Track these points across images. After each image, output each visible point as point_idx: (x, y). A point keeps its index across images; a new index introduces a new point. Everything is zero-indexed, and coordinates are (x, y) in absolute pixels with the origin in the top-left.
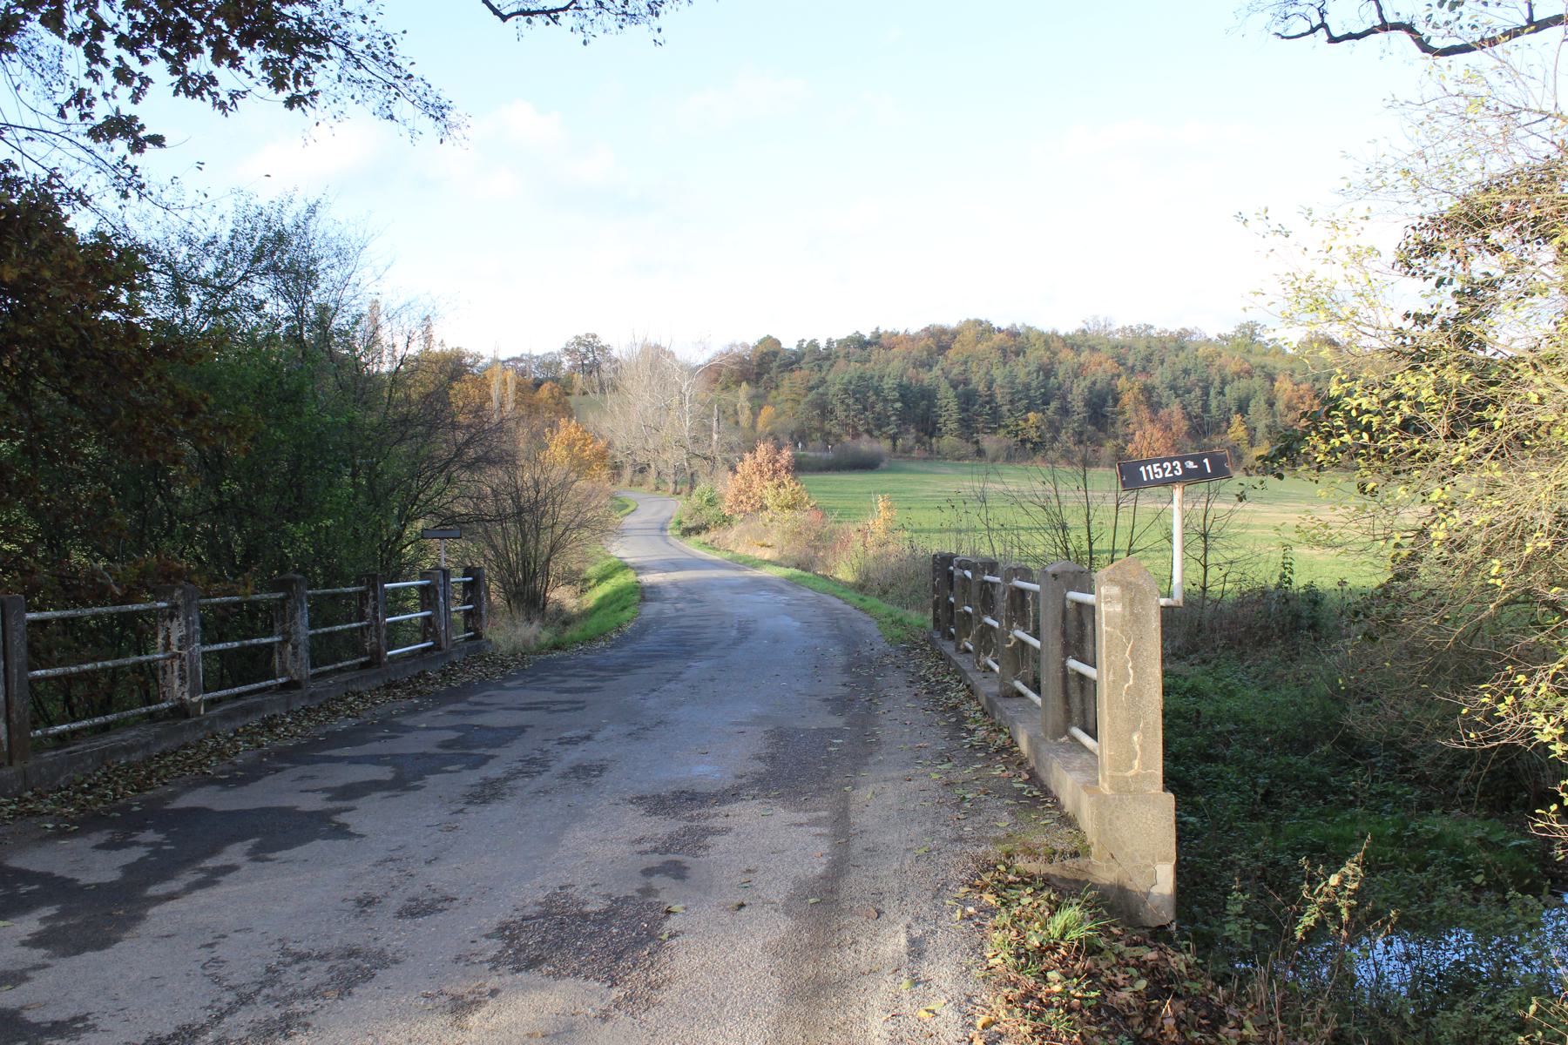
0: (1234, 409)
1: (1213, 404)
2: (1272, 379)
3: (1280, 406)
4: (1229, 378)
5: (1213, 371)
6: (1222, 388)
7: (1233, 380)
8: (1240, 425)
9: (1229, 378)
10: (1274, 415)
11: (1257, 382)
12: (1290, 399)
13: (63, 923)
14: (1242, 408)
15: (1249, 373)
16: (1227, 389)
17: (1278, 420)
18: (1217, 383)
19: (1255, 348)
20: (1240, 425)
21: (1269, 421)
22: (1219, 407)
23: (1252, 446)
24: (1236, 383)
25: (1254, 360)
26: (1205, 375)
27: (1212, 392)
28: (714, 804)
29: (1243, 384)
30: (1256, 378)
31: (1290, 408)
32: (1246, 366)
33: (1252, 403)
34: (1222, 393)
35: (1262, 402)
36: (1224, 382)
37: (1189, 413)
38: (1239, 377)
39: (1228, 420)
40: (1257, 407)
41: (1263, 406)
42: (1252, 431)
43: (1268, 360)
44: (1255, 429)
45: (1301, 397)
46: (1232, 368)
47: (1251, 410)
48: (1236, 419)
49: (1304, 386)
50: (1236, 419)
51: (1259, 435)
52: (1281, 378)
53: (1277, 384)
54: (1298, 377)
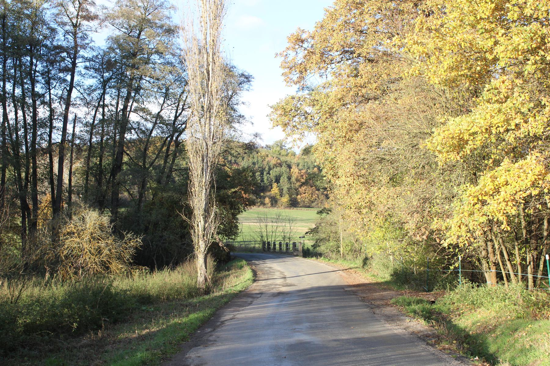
0: (274, 180)
1: (265, 178)
2: (289, 167)
3: (293, 179)
4: (272, 167)
5: (265, 163)
6: (269, 172)
7: (274, 168)
8: (276, 188)
9: (272, 167)
10: (291, 183)
11: (284, 168)
12: (298, 177)
13: (32, 164)
14: (277, 180)
15: (280, 165)
16: (271, 172)
17: (292, 185)
18: (267, 169)
19: (283, 152)
20: (276, 188)
21: (288, 186)
22: (267, 180)
23: (281, 197)
24: (275, 169)
25: (283, 159)
26: (262, 165)
27: (265, 173)
28: (212, 176)
29: (278, 169)
30: (283, 167)
31: (298, 180)
32: (279, 161)
33: (282, 178)
34: (269, 173)
35: (286, 178)
36: (270, 169)
37: (122, 342)
38: (276, 166)
39: (271, 185)
40: (284, 180)
41: (286, 179)
42: (281, 190)
43: (288, 159)
44: (282, 189)
45: (302, 176)
46: (273, 162)
47: (281, 181)
48: (275, 185)
49: (303, 171)
50: (275, 185)
51: (284, 192)
52: (294, 167)
53: (292, 170)
54: (300, 167)
